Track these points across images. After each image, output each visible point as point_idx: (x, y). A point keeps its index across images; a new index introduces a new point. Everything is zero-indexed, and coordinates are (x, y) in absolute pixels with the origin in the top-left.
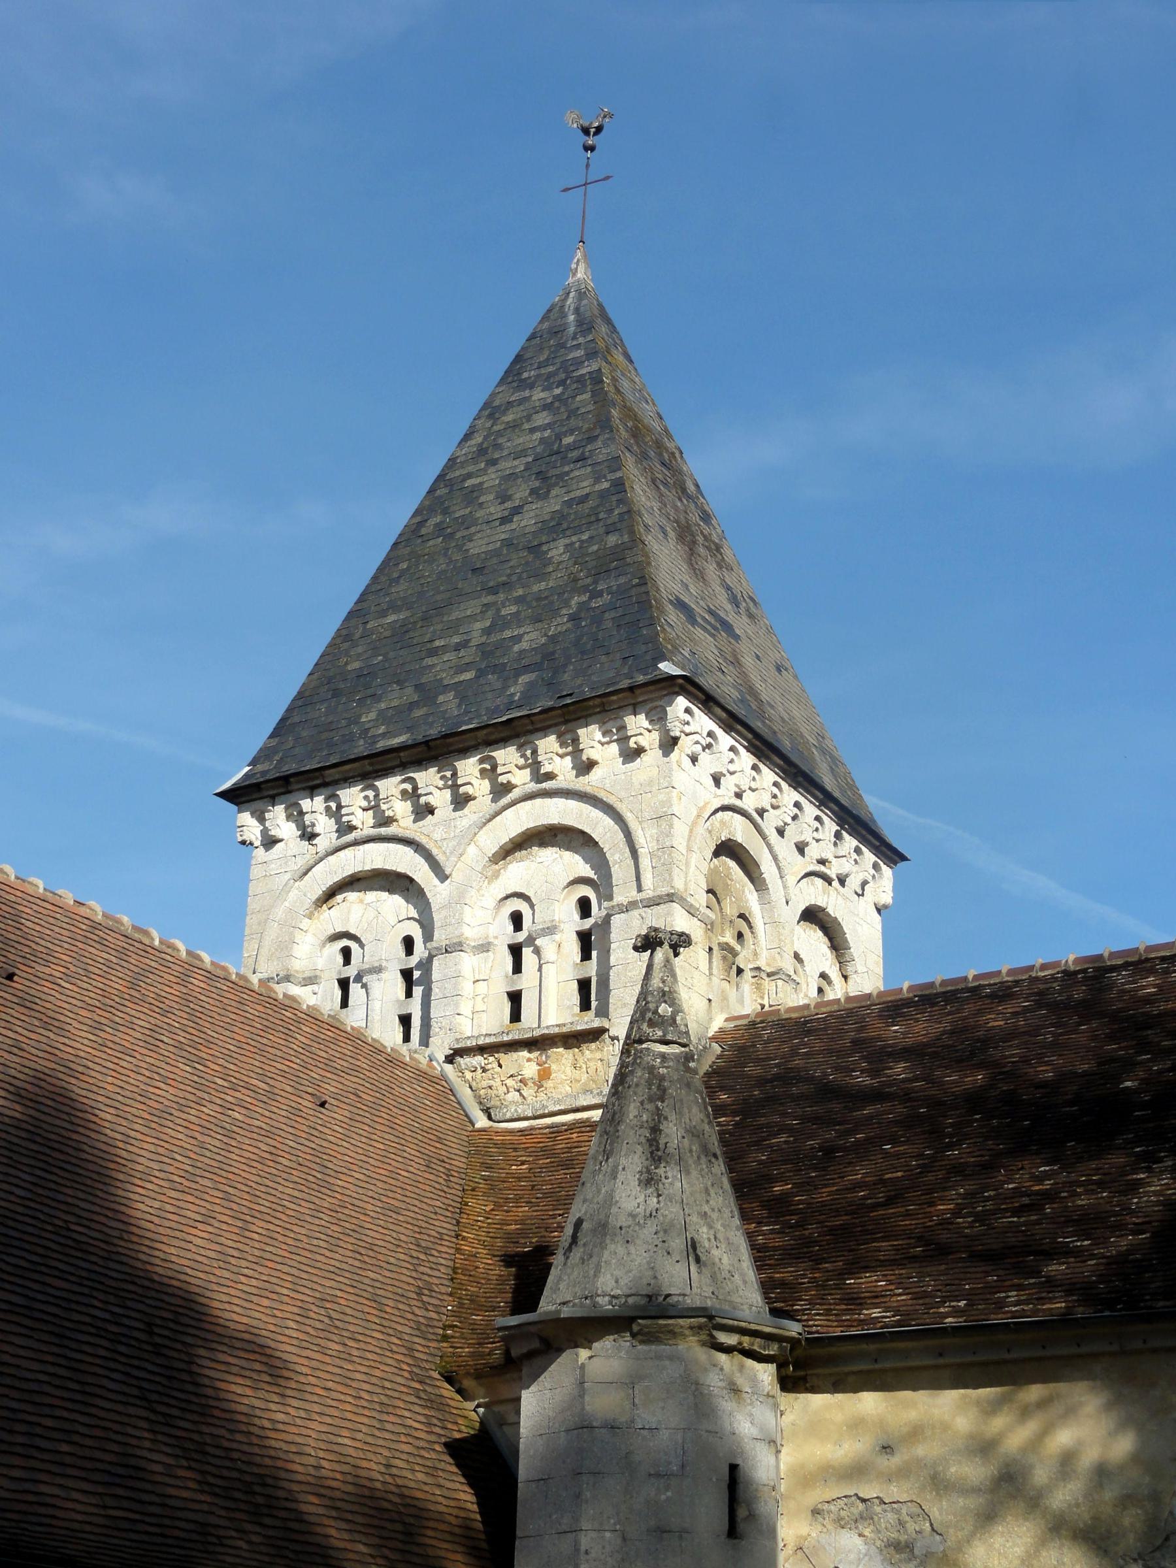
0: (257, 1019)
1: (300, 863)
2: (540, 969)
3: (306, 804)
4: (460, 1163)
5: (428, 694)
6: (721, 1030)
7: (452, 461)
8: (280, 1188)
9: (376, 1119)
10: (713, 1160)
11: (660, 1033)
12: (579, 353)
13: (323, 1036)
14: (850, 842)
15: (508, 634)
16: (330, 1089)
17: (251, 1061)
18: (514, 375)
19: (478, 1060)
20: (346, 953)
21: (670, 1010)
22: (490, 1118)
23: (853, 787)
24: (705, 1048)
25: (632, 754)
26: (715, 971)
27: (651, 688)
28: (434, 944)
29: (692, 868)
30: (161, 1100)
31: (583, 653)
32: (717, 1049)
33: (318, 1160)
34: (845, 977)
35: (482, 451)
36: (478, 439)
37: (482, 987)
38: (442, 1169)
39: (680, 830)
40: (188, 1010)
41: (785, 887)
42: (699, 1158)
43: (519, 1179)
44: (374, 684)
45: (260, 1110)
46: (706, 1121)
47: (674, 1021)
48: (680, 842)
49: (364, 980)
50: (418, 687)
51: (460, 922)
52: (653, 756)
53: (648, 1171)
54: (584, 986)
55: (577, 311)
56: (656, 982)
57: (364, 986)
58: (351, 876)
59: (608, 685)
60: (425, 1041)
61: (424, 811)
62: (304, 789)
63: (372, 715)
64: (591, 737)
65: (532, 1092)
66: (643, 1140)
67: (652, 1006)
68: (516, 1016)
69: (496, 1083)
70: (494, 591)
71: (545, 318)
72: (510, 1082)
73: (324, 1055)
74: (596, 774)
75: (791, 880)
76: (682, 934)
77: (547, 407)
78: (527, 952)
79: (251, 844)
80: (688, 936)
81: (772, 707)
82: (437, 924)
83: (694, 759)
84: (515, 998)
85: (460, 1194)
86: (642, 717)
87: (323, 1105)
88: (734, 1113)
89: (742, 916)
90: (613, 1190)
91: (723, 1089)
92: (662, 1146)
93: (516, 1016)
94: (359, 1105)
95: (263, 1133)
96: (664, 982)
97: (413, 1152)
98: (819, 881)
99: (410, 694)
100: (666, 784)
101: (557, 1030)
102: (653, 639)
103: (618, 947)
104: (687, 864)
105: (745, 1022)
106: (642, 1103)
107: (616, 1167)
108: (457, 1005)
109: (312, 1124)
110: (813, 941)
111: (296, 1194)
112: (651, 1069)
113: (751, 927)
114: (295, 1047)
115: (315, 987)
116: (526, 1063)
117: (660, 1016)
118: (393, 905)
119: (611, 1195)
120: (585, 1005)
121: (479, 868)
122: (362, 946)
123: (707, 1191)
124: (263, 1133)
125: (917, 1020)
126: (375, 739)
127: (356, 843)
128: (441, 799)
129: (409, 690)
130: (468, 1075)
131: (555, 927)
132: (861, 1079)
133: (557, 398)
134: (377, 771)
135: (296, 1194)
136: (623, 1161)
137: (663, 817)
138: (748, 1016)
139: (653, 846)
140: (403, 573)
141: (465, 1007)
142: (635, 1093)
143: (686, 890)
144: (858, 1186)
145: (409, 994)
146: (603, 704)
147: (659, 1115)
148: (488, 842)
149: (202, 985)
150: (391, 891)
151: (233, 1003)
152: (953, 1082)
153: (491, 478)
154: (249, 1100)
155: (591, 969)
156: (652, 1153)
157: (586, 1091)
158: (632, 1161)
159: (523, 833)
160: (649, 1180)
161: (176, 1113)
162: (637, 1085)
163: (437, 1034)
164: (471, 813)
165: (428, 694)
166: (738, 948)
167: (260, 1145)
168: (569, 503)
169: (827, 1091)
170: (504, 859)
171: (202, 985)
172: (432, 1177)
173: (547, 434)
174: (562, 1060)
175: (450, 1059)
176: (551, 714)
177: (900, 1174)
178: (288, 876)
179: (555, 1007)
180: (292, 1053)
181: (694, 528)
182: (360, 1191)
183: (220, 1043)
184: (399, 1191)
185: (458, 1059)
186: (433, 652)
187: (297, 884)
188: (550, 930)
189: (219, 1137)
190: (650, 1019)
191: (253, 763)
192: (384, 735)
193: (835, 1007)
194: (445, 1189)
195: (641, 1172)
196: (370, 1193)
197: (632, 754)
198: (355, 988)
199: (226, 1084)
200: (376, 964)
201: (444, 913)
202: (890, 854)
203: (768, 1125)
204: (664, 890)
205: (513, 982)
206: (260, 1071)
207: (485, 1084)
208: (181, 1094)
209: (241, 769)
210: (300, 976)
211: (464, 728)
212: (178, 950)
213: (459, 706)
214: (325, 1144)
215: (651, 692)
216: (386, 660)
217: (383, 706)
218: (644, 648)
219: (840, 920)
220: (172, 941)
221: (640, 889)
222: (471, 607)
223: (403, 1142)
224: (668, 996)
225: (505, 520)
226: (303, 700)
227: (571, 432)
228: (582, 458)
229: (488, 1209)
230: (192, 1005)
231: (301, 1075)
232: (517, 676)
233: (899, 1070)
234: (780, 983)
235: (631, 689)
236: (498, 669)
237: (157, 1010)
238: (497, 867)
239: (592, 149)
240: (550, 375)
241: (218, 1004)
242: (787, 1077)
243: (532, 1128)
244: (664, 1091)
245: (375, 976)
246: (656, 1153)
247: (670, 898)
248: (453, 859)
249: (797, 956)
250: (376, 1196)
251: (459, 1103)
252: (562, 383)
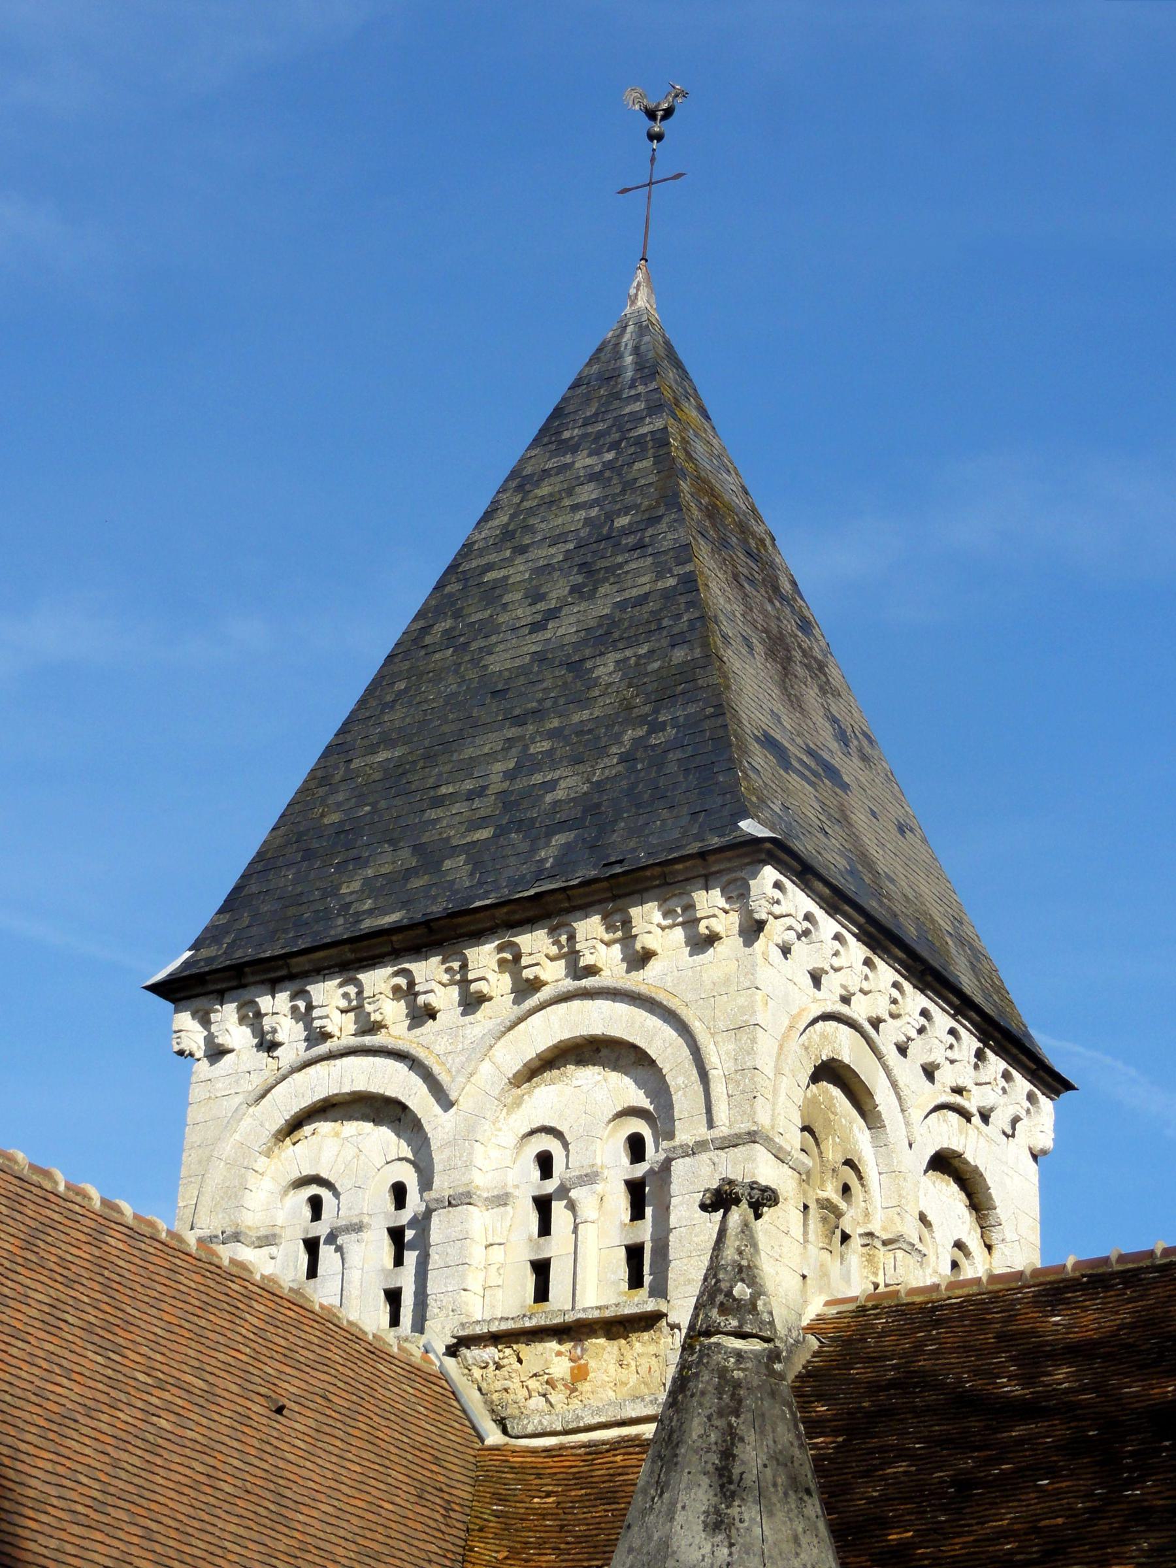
0: (193, 1293)
1: (257, 1082)
2: (575, 1231)
3: (265, 1003)
4: (463, 1492)
5: (430, 858)
6: (820, 1318)
7: (467, 550)
8: (220, 1524)
9: (350, 1430)
10: (806, 1498)
11: (735, 1323)
12: (639, 406)
13: (281, 1317)
14: (996, 1064)
15: (538, 778)
16: (290, 1388)
17: (183, 1349)
18: (551, 434)
19: (490, 1353)
20: (316, 1204)
21: (749, 1291)
22: (505, 1431)
23: (1000, 990)
24: (797, 1342)
25: (702, 942)
26: (812, 1237)
27: (729, 854)
28: (433, 1194)
29: (782, 1098)
30: (63, 1401)
31: (638, 806)
32: (813, 1343)
33: (272, 1487)
34: (989, 1247)
35: (507, 535)
36: (502, 518)
37: (497, 1254)
38: (438, 1501)
39: (766, 1046)
40: (101, 1279)
41: (907, 1124)
42: (786, 1494)
43: (544, 1516)
44: (359, 843)
45: (195, 1417)
46: (796, 1443)
47: (755, 1306)
48: (766, 1064)
49: (339, 1241)
50: (418, 849)
51: (469, 1165)
52: (730, 945)
53: (717, 1512)
54: (634, 1253)
55: (636, 350)
56: (729, 1254)
57: (339, 1249)
58: (325, 1100)
59: (671, 850)
60: (419, 1325)
61: (422, 1015)
62: (263, 982)
63: (356, 886)
64: (649, 920)
65: (562, 1397)
66: (710, 1467)
67: (724, 1286)
68: (542, 1294)
69: (514, 1385)
70: (519, 721)
71: (594, 359)
72: (533, 1384)
73: (283, 1342)
74: (654, 968)
75: (916, 1114)
76: (766, 1189)
77: (593, 477)
78: (558, 1207)
79: (191, 1055)
80: (773, 1191)
81: (892, 881)
82: (438, 1168)
83: (786, 950)
84: (541, 1269)
85: (462, 1535)
86: (716, 893)
87: (280, 1410)
88: (836, 1432)
89: (849, 1163)
90: (668, 1537)
91: (821, 1397)
92: (735, 1477)
93: (542, 1294)
94: (328, 1412)
95: (198, 1447)
96: (740, 1253)
97: (401, 1477)
98: (953, 1117)
99: (406, 858)
100: (747, 984)
101: (596, 1314)
102: (732, 789)
103: (682, 1204)
104: (775, 1092)
105: (852, 1306)
106: (709, 1418)
107: (673, 1504)
108: (463, 1277)
109: (264, 1437)
110: (945, 1197)
111: (241, 1531)
112: (723, 1373)
113: (860, 1178)
114: (244, 1332)
115: (273, 1250)
116: (554, 1358)
117: (735, 1299)
118: (380, 1140)
119: (665, 1543)
120: (636, 1281)
121: (496, 1093)
122: (337, 1194)
123: (796, 1540)
124: (198, 1447)
125: (1085, 1309)
126: (358, 917)
127: (331, 1056)
128: (445, 998)
129: (405, 853)
130: (477, 1373)
131: (597, 1174)
132: (1009, 1388)
133: (609, 465)
134: (361, 960)
135: (241, 1531)
136: (683, 1498)
137: (743, 1028)
138: (855, 1299)
139: (730, 1066)
140: (401, 693)
141: (475, 1281)
142: (701, 1405)
143: (773, 1128)
144: (1004, 1535)
145: (399, 1261)
146: (664, 875)
147: (732, 1437)
148: (508, 1057)
149: (121, 1246)
150: (377, 1121)
151: (163, 1272)
152: (1135, 1395)
153: (519, 571)
154: (180, 1402)
155: (645, 1232)
156: (722, 1486)
157: (636, 1398)
158: (695, 1497)
159: (555, 1047)
160: (718, 1524)
161: (82, 1419)
162: (703, 1393)
163: (436, 1316)
165: (430, 858)
166: (843, 1205)
167: (195, 1464)
168: (621, 606)
169: (965, 1403)
170: (529, 1080)
171: (121, 1246)
172: (425, 1511)
173: (594, 512)
174: (602, 1354)
175: (452, 1351)
176: (594, 887)
177: (1060, 1521)
178: (238, 1100)
179: (594, 1283)
180: (239, 1339)
181: (789, 640)
182: (329, 1529)
183: (143, 1325)
184: (381, 1529)
185: (464, 1351)
186: (438, 802)
187: (251, 1109)
188: (589, 1178)
189: (139, 1452)
190: (722, 1304)
191: (195, 946)
192: (370, 912)
193: (975, 1289)
194: (443, 1528)
195: (707, 1513)
196: (342, 1533)
197: (702, 942)
198: (326, 1253)
199: (149, 1381)
200: (355, 1220)
201: (447, 1153)
202: (1050, 1081)
203: (883, 1449)
204: (744, 1127)
205: (539, 1248)
206: (196, 1364)
207: (498, 1385)
208: (89, 1393)
209: (180, 955)
210: (254, 1234)
211: (478, 904)
212: (90, 1199)
213: (472, 874)
214: (281, 1464)
215: (729, 860)
216: (374, 812)
217: (370, 872)
218: (719, 801)
219: (982, 1169)
220: (82, 1185)
221: (711, 1125)
222: (490, 743)
223: (387, 1463)
224: (746, 1272)
226: (264, 863)
227: (626, 510)
228: (641, 546)
229: (500, 1556)
230: (106, 1273)
231: (251, 1369)
232: (549, 835)
233: (1061, 1376)
234: (900, 1254)
235: (702, 855)
236: (521, 825)
237: (60, 1279)
238: (519, 1091)
239: (659, 137)
240: (601, 435)
241: (142, 1271)
242: (910, 1381)
243: (562, 1447)
244: (740, 1401)
245: (353, 1236)
246: (727, 1483)
247: (752, 1137)
248: (461, 1079)
249: (923, 1218)
250: (349, 1536)
251: (464, 1411)
252: (615, 446)
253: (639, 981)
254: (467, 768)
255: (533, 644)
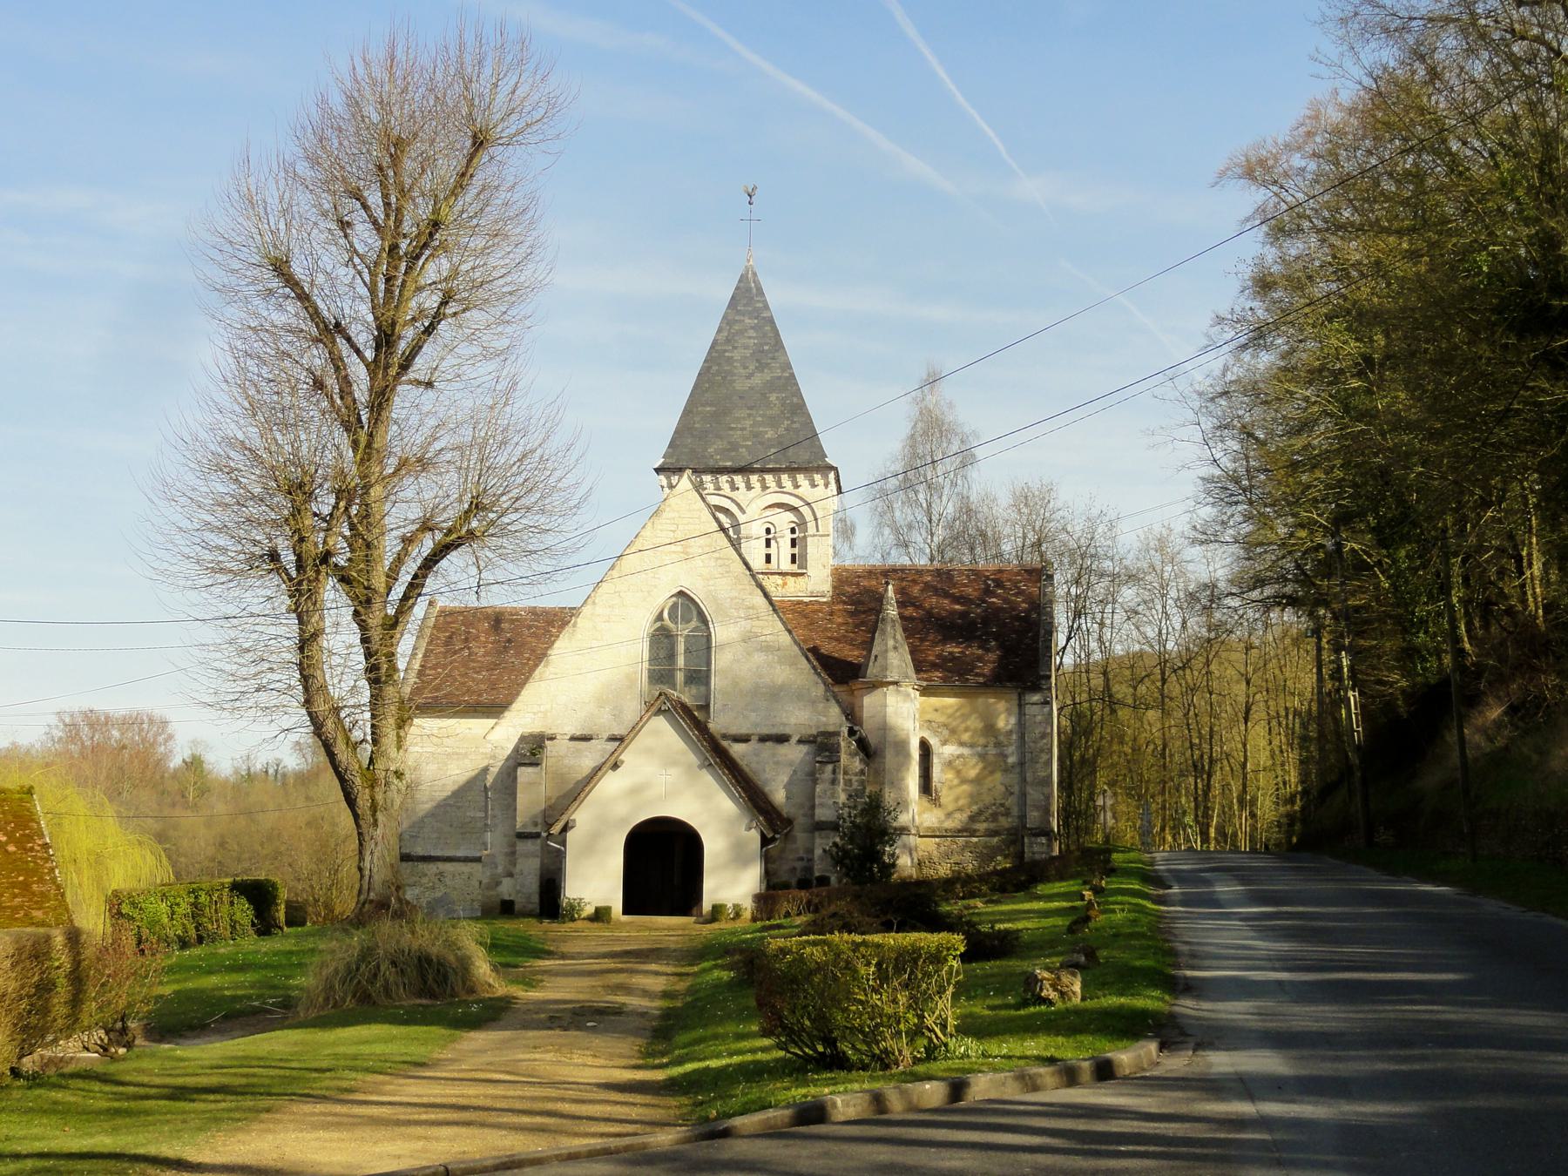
5: (734, 447)
7: (715, 343)
35: (728, 341)
54: (793, 556)
64: (800, 478)
70: (750, 408)
116: (778, 580)
120: (793, 561)
128: (742, 485)
153: (736, 355)
155: (796, 551)
164: (752, 493)
165: (734, 447)
174: (790, 580)
197: (814, 485)
225: (749, 377)
226: (678, 433)
253: (796, 492)
254: (738, 420)
255: (748, 383)
